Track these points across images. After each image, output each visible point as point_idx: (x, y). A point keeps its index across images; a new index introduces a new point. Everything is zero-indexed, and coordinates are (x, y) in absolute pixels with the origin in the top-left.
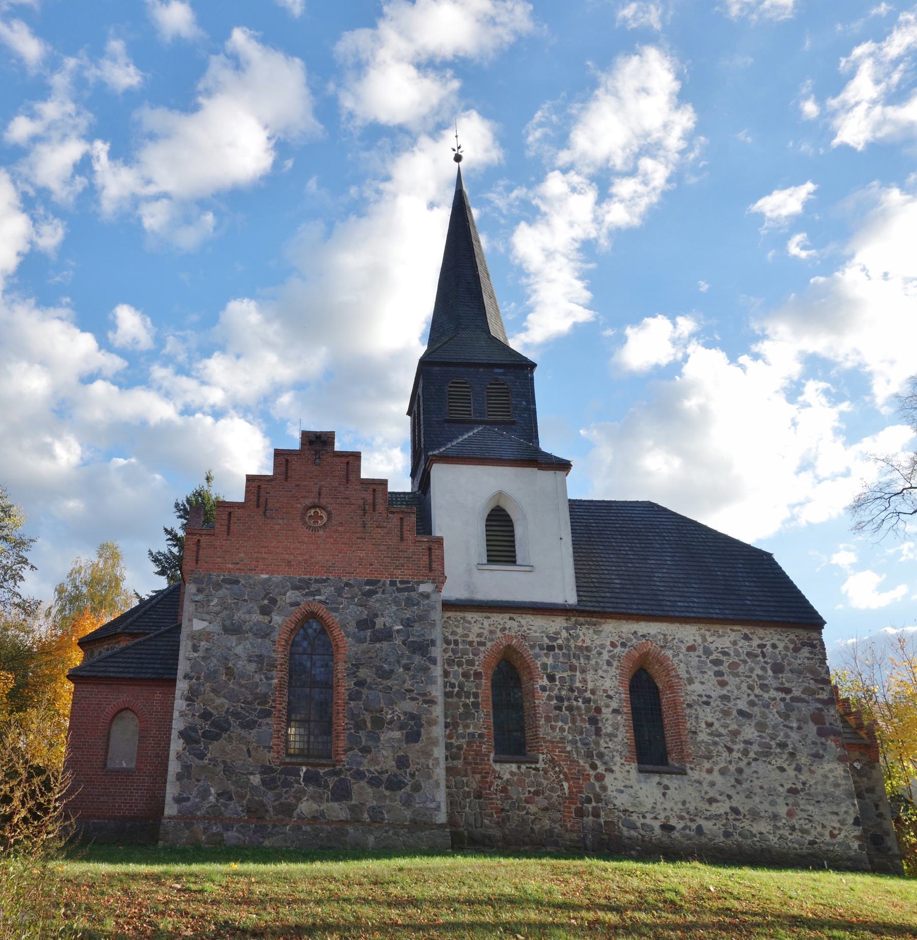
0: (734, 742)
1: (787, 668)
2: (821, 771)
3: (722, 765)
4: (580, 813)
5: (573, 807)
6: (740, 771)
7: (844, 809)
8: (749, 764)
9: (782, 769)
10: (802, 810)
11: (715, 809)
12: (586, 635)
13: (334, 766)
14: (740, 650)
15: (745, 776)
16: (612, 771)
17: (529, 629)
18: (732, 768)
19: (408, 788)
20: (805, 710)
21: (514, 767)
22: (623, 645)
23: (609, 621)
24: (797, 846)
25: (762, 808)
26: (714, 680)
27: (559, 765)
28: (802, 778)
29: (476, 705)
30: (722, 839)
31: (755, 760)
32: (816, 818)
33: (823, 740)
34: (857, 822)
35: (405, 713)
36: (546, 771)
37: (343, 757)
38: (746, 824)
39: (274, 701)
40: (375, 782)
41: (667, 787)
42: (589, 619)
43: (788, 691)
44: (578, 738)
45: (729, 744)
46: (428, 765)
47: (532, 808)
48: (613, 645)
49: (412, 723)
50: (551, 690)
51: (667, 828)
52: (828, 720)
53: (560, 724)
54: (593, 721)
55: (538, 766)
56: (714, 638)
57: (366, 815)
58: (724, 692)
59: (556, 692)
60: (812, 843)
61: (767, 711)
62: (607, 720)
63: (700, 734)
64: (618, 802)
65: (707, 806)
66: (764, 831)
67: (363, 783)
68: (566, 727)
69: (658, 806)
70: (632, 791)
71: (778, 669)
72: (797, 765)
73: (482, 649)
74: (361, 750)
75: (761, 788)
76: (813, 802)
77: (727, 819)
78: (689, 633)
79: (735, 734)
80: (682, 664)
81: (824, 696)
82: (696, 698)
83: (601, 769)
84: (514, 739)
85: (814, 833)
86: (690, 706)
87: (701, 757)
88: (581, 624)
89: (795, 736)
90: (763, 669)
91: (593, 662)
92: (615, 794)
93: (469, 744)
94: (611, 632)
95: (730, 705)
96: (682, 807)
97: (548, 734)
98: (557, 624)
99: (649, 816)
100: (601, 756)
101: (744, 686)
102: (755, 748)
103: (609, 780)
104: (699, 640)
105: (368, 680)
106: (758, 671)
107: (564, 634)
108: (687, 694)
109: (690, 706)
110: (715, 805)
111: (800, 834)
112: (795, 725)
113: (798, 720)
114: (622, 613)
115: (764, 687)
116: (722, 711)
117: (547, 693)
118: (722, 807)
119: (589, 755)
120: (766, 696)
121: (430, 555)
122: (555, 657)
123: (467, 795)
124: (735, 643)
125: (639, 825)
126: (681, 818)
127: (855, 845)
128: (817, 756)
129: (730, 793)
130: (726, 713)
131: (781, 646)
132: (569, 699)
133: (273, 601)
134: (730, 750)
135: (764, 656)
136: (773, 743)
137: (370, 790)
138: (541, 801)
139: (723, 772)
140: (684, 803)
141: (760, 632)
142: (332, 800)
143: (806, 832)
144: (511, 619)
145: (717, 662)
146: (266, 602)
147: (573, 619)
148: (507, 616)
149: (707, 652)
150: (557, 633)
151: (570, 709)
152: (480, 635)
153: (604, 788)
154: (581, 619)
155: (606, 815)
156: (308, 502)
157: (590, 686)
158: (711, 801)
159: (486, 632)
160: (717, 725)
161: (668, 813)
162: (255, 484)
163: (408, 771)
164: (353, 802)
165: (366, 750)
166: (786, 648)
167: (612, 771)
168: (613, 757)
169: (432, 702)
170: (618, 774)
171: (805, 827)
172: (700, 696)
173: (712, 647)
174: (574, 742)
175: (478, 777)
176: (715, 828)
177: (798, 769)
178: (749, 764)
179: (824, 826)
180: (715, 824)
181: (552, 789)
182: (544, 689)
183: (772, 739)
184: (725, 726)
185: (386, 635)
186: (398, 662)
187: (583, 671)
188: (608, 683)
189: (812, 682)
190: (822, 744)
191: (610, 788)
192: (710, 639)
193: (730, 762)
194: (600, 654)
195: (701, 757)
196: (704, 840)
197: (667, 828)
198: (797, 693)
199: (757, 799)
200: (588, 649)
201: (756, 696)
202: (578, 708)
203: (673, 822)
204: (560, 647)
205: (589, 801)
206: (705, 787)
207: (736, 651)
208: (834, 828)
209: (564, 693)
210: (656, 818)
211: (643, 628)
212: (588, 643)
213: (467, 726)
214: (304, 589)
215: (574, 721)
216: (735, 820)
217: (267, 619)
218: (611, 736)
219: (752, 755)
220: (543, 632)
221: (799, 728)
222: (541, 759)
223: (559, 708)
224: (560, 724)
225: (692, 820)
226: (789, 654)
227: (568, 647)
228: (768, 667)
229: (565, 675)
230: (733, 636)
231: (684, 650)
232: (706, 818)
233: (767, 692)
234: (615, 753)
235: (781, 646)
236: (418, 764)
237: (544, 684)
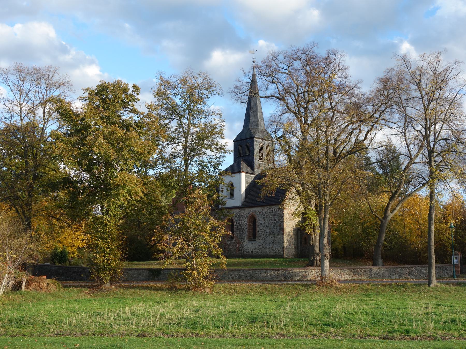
12: (243, 212)
43: (275, 220)
51: (252, 252)
54: (242, 231)
71: (275, 215)
78: (260, 209)
79: (265, 231)
89: (275, 230)
102: (268, 234)
115: (272, 220)
118: (261, 247)
119: (241, 239)
128: (279, 234)
130: (264, 227)
141: (272, 207)
145: (264, 215)
158: (260, 246)
177: (275, 238)
188: (245, 222)
197: (252, 252)
198: (277, 220)
230: (268, 209)
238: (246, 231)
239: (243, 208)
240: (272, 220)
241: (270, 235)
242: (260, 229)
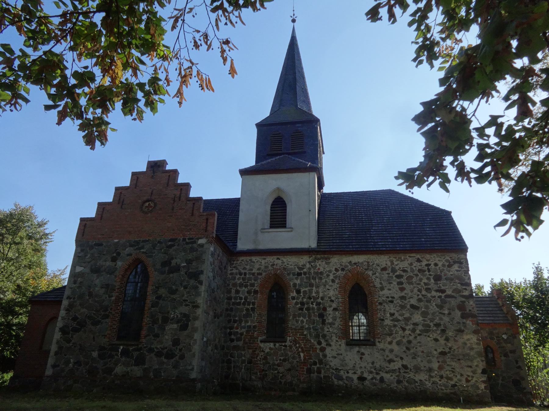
0: (407, 325)
1: (444, 277)
2: (461, 341)
3: (398, 339)
4: (309, 371)
5: (305, 368)
7: (475, 364)
8: (416, 337)
9: (436, 340)
10: (448, 365)
11: (392, 366)
12: (321, 265)
13: (138, 345)
14: (414, 268)
15: (412, 345)
16: (330, 345)
17: (288, 264)
18: (405, 340)
19: (177, 357)
20: (453, 303)
21: (272, 345)
22: (343, 270)
23: (335, 256)
24: (443, 388)
25: (422, 365)
26: (397, 287)
27: (299, 343)
28: (449, 345)
29: (253, 309)
30: (396, 385)
31: (419, 335)
32: (458, 370)
33: (464, 321)
34: (484, 372)
35: (181, 314)
36: (291, 347)
37: (144, 341)
38: (411, 375)
39: (111, 309)
40: (159, 354)
41: (363, 354)
42: (323, 256)
44: (311, 326)
45: (404, 326)
46: (190, 344)
47: (281, 369)
48: (336, 270)
49: (184, 319)
50: (298, 298)
51: (362, 379)
52: (468, 308)
54: (321, 316)
55: (286, 344)
56: (399, 262)
57: (151, 374)
58: (403, 294)
59: (300, 300)
60: (454, 386)
61: (429, 304)
62: (330, 314)
63: (386, 321)
64: (332, 364)
65: (387, 365)
66: (423, 379)
67: (152, 355)
68: (305, 321)
69: (357, 366)
70: (341, 357)
71: (438, 278)
72: (446, 337)
73: (260, 277)
74: (154, 336)
75: (423, 352)
76: (455, 360)
77: (400, 372)
78: (383, 260)
79: (407, 320)
80: (377, 279)
81: (466, 293)
82: (384, 299)
83: (324, 344)
84: (276, 329)
85: (455, 379)
86: (380, 304)
87: (386, 334)
88: (319, 259)
89: (446, 319)
90: (428, 279)
91: (324, 281)
92: (331, 359)
93: (247, 332)
94: (336, 263)
95: (406, 302)
96: (371, 365)
97: (293, 325)
98: (304, 260)
100: (324, 336)
101: (416, 290)
102: (420, 327)
103: (328, 351)
104: (389, 264)
105: (163, 295)
107: (308, 266)
108: (379, 297)
109: (380, 304)
110: (392, 364)
111: (446, 380)
112: (446, 312)
113: (449, 309)
114: (341, 251)
116: (401, 306)
117: (295, 301)
118: (397, 365)
119: (317, 336)
120: (429, 295)
121: (207, 223)
122: (302, 280)
123: (243, 362)
124: (411, 264)
125: (344, 377)
126: (371, 372)
127: (482, 386)
128: (460, 331)
129: (402, 356)
131: (440, 264)
132: (308, 303)
133: (119, 254)
134: (404, 330)
135: (429, 270)
136: (431, 324)
137: (156, 359)
138: (287, 365)
139: (398, 343)
140: (373, 363)
141: (428, 256)
142: (134, 366)
143: (451, 379)
144: (278, 259)
146: (115, 255)
147: (314, 256)
148: (276, 257)
149: (394, 271)
150: (304, 265)
151: (308, 309)
152: (259, 269)
153: (325, 356)
154: (319, 256)
155: (325, 372)
156: (145, 198)
157: (321, 295)
158: (390, 361)
159: (263, 267)
160: (397, 315)
161: (363, 370)
162: (120, 191)
163: (178, 347)
164: (146, 366)
165: (157, 336)
166: (444, 265)
167: (330, 345)
168: (332, 336)
169: (197, 307)
170: (334, 347)
171: (450, 376)
172: (388, 297)
173: (397, 268)
174: (309, 329)
175: (251, 351)
176: (392, 378)
177: (447, 339)
178: (416, 337)
179: (462, 375)
180: (392, 376)
181: (294, 358)
182: (293, 298)
183: (431, 321)
184: (402, 315)
185: (177, 269)
186: (181, 284)
187: (318, 287)
189: (459, 285)
190: (464, 323)
191: (328, 355)
192: (396, 263)
193: (404, 337)
194: (328, 276)
195: (386, 334)
196: (384, 386)
197: (362, 379)
198: (449, 292)
199: (419, 359)
200: (321, 273)
201: (423, 295)
202: (313, 308)
203: (365, 375)
204: (305, 273)
205: (315, 363)
206: (387, 352)
207: (412, 269)
208: (469, 376)
209: (305, 300)
210: (355, 373)
211: (356, 259)
212: (322, 269)
213: (247, 322)
214: (135, 246)
215: (310, 316)
216: (404, 372)
217: (114, 263)
218: (331, 324)
219: (418, 332)
220: (296, 265)
221: (449, 314)
222: (288, 340)
223: (301, 309)
224: (301, 318)
225: (377, 374)
226: (445, 268)
227: (310, 273)
229: (307, 289)
230: (410, 260)
231: (379, 270)
232: (387, 372)
233: (430, 293)
234: (333, 334)
235: (440, 264)
236: (185, 343)
237: (294, 295)
239: (324, 252)
240: (428, 290)
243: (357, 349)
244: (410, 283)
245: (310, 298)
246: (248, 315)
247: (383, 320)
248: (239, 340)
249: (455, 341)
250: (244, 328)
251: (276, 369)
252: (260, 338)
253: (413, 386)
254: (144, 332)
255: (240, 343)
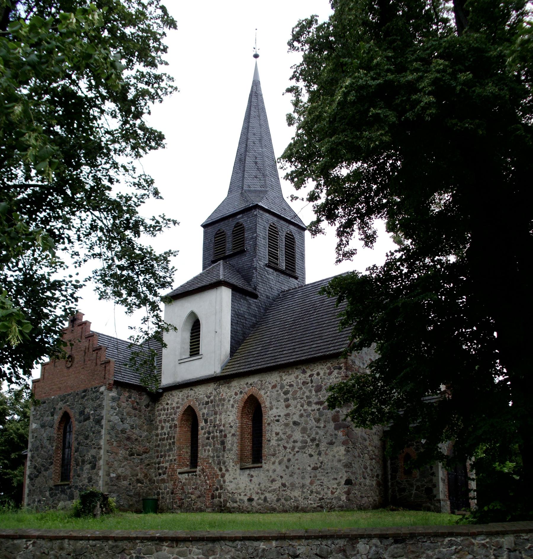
1: (324, 387)
2: (332, 453)
6: (289, 460)
9: (311, 456)
10: (318, 480)
15: (291, 463)
18: (285, 459)
25: (297, 481)
32: (325, 483)
33: (336, 432)
38: (288, 493)
41: (252, 476)
47: (193, 497)
48: (236, 394)
51: (250, 500)
53: (208, 447)
54: (223, 443)
64: (229, 488)
66: (297, 496)
69: (248, 488)
73: (178, 410)
75: (299, 469)
86: (269, 424)
87: (270, 455)
89: (321, 433)
90: (310, 391)
91: (225, 407)
92: (228, 484)
95: (290, 419)
96: (257, 486)
98: (210, 388)
99: (243, 494)
101: (299, 406)
102: (299, 444)
103: (227, 476)
106: (308, 394)
107: (214, 393)
110: (274, 483)
112: (322, 425)
115: (309, 404)
118: (277, 485)
120: (310, 409)
125: (238, 500)
126: (258, 493)
128: (331, 443)
130: (287, 425)
132: (213, 432)
134: (285, 448)
138: (197, 493)
140: (259, 484)
150: (211, 393)
151: (213, 438)
153: (224, 482)
157: (223, 423)
158: (273, 481)
159: (180, 400)
172: (275, 416)
174: (213, 457)
177: (319, 454)
178: (294, 455)
188: (231, 417)
190: (335, 435)
191: (227, 481)
192: (284, 378)
194: (229, 401)
195: (270, 455)
197: (250, 500)
199: (295, 476)
200: (224, 400)
202: (217, 437)
206: (271, 473)
210: (245, 495)
213: (169, 456)
215: (214, 446)
216: (284, 490)
219: (297, 449)
221: (325, 427)
224: (208, 447)
225: (262, 494)
228: (313, 389)
229: (212, 418)
233: (311, 406)
238: (232, 443)
241: (303, 448)
242: (272, 432)
243: (247, 472)
244: (295, 399)
245: (215, 427)
246: (170, 450)
247: (269, 441)
248: (164, 473)
249: (326, 454)
250: (167, 461)
251: (190, 497)
252: (179, 470)
253: (289, 502)
254: (72, 474)
255: (165, 477)
